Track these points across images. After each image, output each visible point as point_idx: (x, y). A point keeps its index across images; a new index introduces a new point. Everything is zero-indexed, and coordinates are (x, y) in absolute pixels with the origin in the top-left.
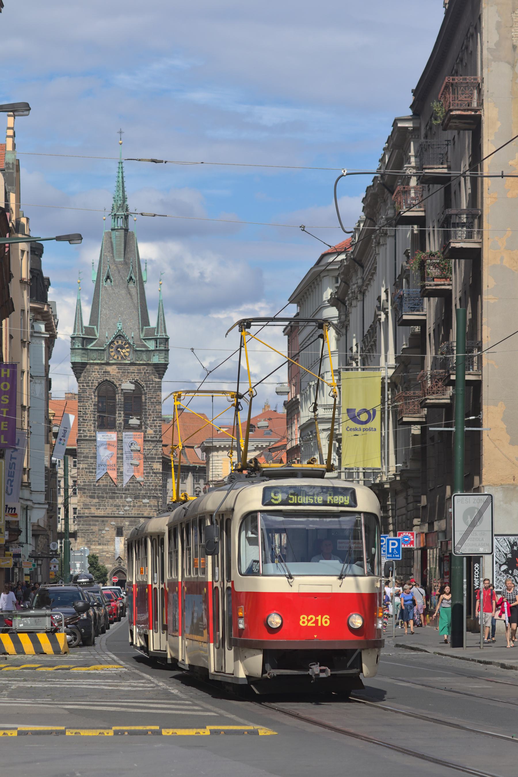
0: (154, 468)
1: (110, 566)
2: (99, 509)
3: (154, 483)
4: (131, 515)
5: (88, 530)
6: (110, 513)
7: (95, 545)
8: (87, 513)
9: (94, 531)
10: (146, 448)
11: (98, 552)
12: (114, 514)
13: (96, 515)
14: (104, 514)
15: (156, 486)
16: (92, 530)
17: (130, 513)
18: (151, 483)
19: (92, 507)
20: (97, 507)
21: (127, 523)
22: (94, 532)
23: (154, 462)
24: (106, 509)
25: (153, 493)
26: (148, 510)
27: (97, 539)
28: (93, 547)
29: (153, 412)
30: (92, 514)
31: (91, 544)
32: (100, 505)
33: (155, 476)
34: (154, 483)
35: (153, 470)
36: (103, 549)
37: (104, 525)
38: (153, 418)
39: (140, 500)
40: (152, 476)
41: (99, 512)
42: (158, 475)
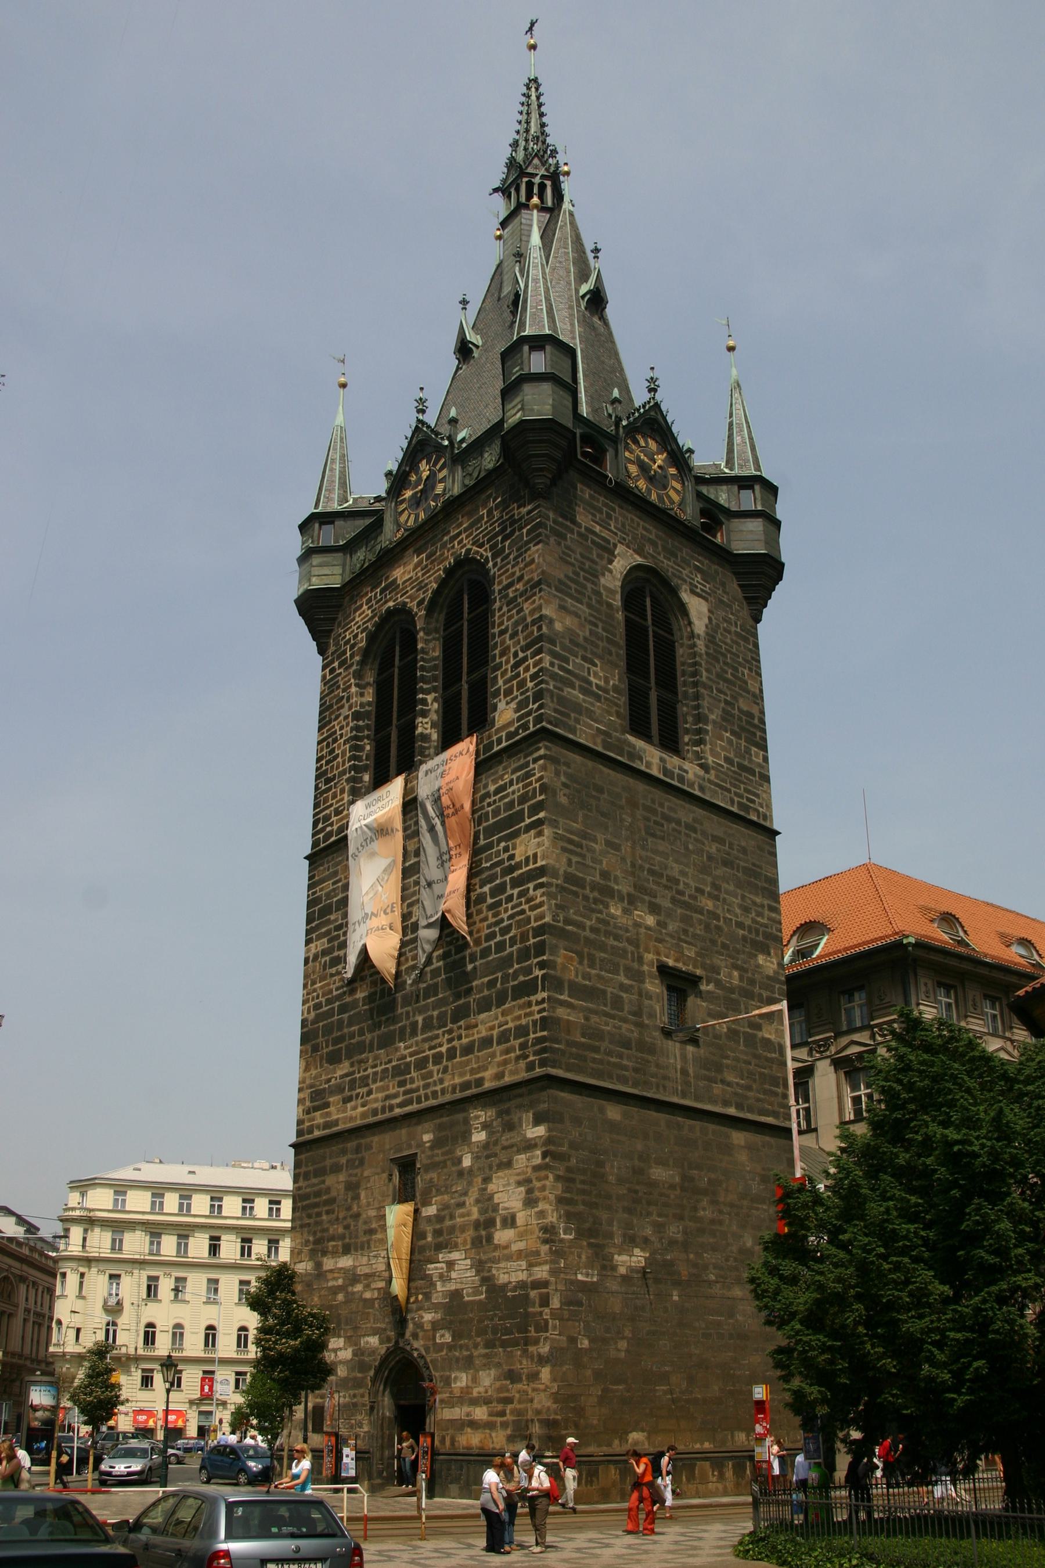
0: (517, 859)
1: (373, 1341)
2: (349, 1099)
3: (519, 925)
4: (441, 1100)
5: (318, 1194)
6: (378, 1105)
7: (335, 1254)
8: (318, 1127)
9: (334, 1193)
10: (492, 788)
11: (340, 1282)
12: (391, 1108)
13: (341, 1127)
14: (364, 1115)
15: (524, 937)
16: (328, 1190)
17: (438, 1088)
18: (508, 929)
19: (331, 1099)
20: (347, 1093)
21: (427, 1137)
22: (333, 1201)
23: (516, 834)
24: (370, 1093)
25: (515, 975)
26: (499, 1059)
27: (341, 1230)
28: (328, 1263)
29: (512, 637)
30: (336, 1123)
31: (324, 1253)
32: (352, 1085)
33: (521, 895)
34: (519, 925)
35: (511, 869)
36: (355, 1267)
37: (362, 1162)
38: (516, 655)
39: (472, 1020)
40: (510, 898)
41: (349, 1113)
42: (531, 885)
